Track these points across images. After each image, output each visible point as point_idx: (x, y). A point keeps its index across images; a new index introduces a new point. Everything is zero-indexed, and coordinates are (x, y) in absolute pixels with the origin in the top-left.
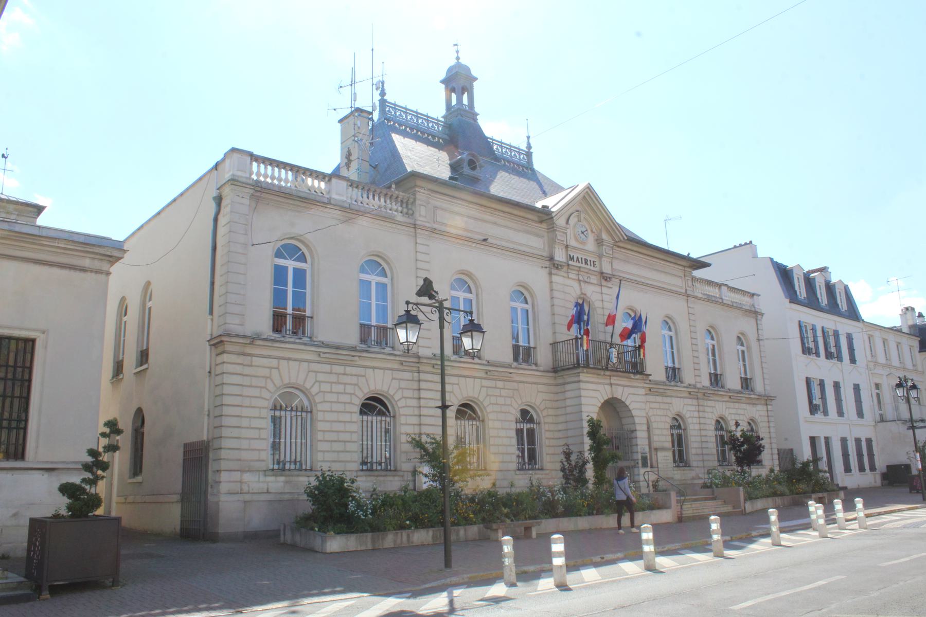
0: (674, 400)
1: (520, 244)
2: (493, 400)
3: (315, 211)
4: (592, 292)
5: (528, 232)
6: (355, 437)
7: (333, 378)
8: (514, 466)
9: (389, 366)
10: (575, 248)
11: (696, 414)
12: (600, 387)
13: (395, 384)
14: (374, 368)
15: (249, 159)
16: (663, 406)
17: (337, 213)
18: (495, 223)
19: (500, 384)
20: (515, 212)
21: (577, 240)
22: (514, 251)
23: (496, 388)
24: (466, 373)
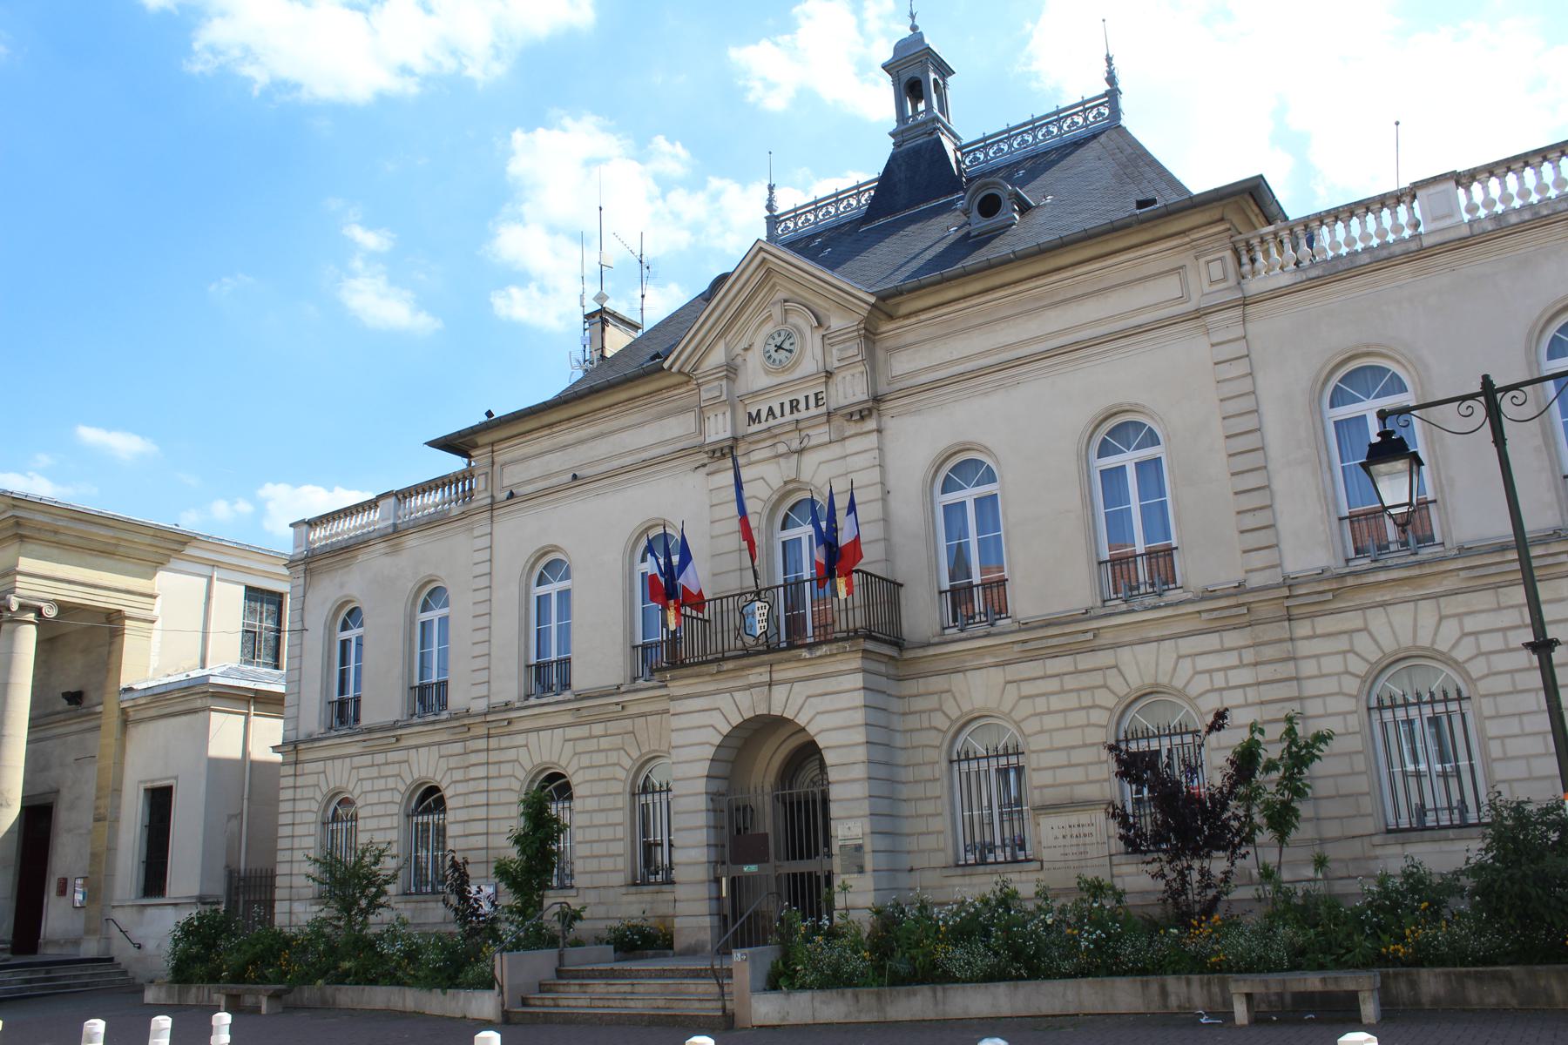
0: (1125, 654)
1: (644, 449)
2: (585, 760)
3: (362, 556)
4: (828, 468)
5: (661, 417)
6: (620, 832)
7: (374, 772)
8: (620, 879)
9: (437, 739)
10: (755, 394)
11: (1246, 676)
12: (723, 701)
13: (443, 764)
14: (417, 747)
15: (305, 527)
16: (1070, 682)
17: (381, 547)
18: (602, 435)
19: (598, 729)
20: (641, 390)
21: (767, 372)
22: (647, 464)
23: (591, 737)
24: (540, 723)
